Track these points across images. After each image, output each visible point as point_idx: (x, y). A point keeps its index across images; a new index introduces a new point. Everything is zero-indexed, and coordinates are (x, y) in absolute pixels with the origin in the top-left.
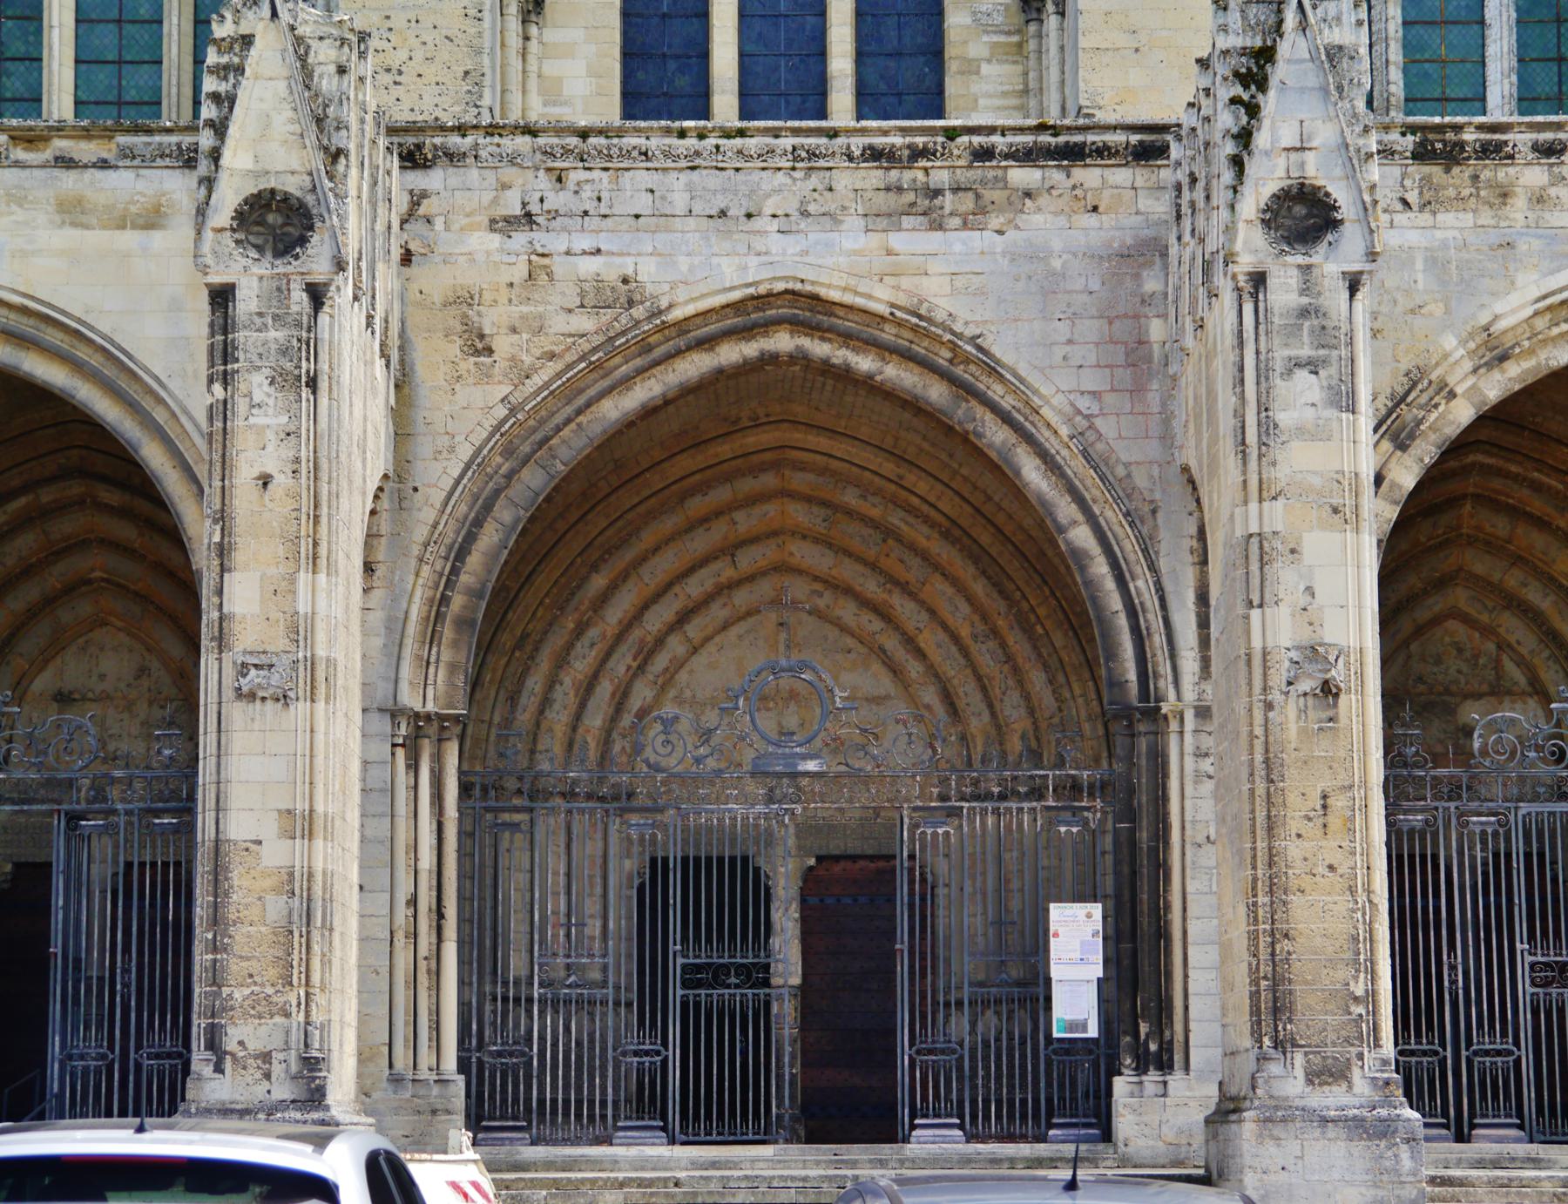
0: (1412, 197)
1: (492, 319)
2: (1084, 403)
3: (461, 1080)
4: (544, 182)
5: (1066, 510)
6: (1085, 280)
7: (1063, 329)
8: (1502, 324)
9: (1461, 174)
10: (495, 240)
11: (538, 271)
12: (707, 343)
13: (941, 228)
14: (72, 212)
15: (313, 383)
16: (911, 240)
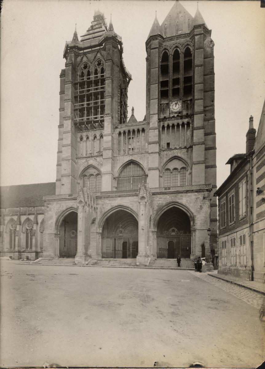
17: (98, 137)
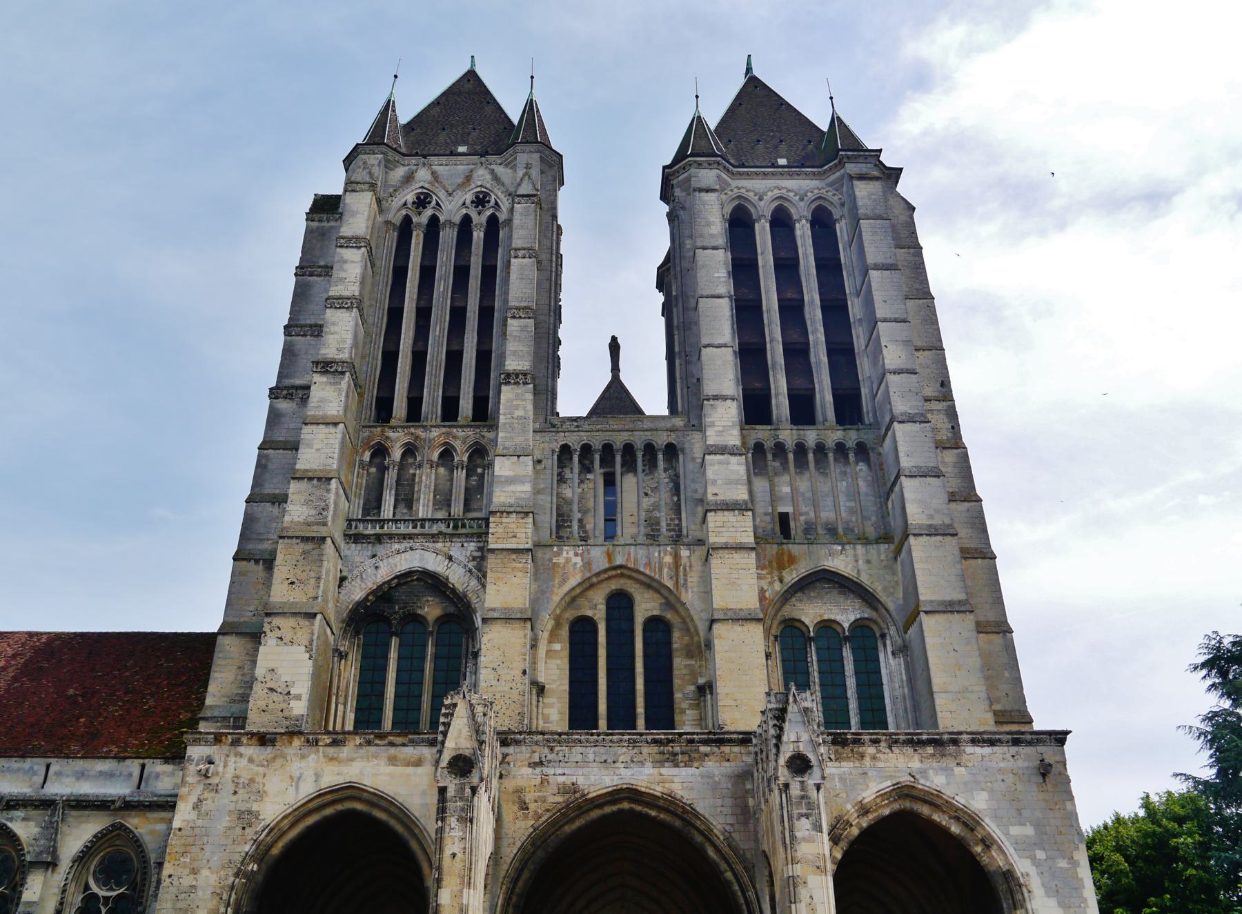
0: (832, 757)
1: (529, 797)
2: (728, 828)
4: (546, 750)
5: (723, 866)
6: (726, 785)
7: (719, 802)
8: (866, 801)
9: (848, 749)
11: (544, 781)
12: (601, 806)
13: (678, 766)
14: (393, 761)
16: (668, 771)
17: (462, 456)
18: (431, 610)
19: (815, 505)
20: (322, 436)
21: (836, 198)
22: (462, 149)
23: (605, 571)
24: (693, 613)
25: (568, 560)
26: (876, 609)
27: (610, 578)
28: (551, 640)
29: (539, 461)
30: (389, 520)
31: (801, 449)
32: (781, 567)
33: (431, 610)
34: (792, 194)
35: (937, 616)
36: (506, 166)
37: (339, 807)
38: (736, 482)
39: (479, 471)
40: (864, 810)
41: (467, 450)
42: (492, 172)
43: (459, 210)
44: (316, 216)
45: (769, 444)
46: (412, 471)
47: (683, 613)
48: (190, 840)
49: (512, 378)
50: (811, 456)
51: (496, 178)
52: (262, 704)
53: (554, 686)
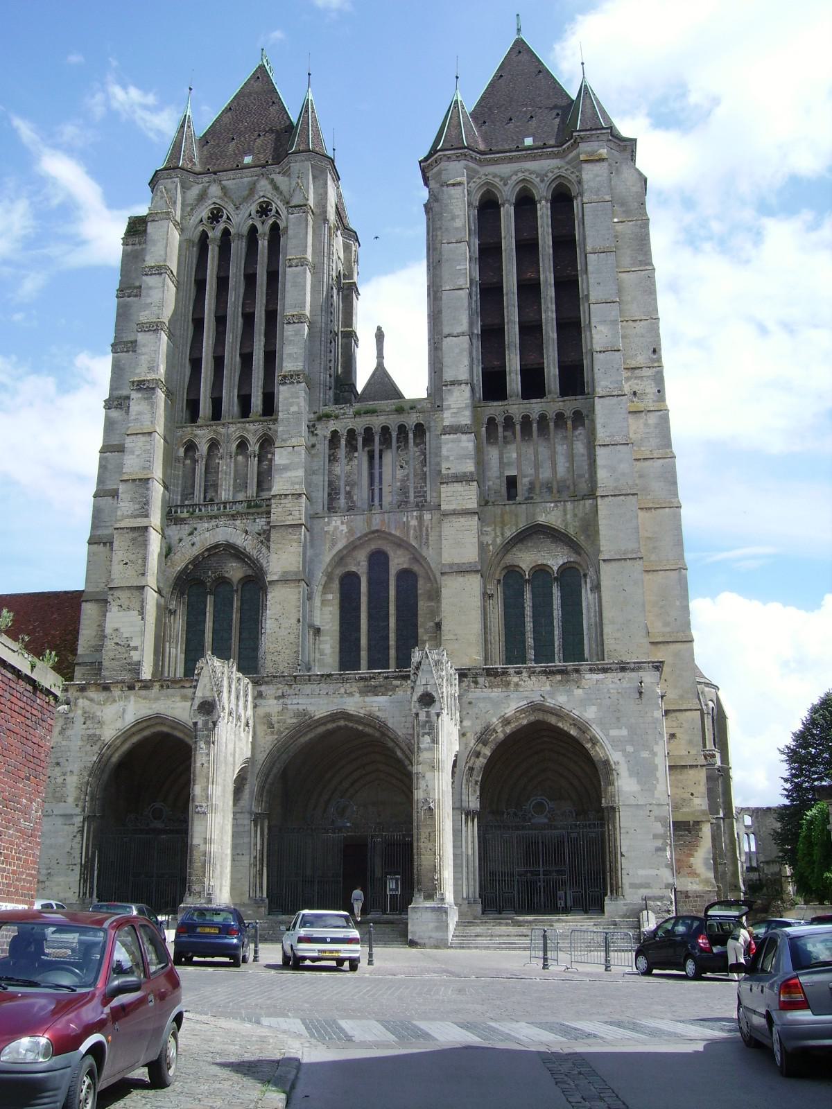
0: (487, 685)
1: (274, 719)
2: (408, 737)
3: (267, 901)
8: (507, 715)
10: (276, 701)
11: (285, 709)
12: (324, 724)
15: (213, 743)
17: (254, 447)
18: (235, 571)
19: (537, 467)
20: (140, 444)
21: (573, 176)
22: (248, 160)
23: (366, 535)
24: (433, 565)
25: (336, 528)
26: (579, 554)
27: (369, 540)
28: (324, 593)
29: (313, 446)
30: (199, 505)
31: (526, 422)
32: (503, 524)
33: (235, 571)
34: (533, 176)
35: (614, 564)
36: (284, 174)
37: (154, 730)
38: (465, 457)
39: (269, 456)
40: (506, 722)
41: (258, 441)
42: (272, 182)
43: (245, 222)
44: (130, 241)
45: (500, 420)
46: (217, 461)
47: (425, 565)
48: (59, 754)
49: (290, 378)
50: (535, 426)
51: (276, 188)
52: (111, 654)
53: (327, 627)
